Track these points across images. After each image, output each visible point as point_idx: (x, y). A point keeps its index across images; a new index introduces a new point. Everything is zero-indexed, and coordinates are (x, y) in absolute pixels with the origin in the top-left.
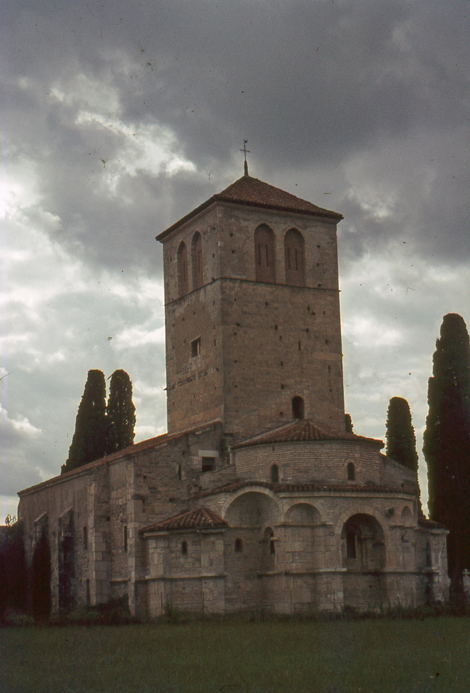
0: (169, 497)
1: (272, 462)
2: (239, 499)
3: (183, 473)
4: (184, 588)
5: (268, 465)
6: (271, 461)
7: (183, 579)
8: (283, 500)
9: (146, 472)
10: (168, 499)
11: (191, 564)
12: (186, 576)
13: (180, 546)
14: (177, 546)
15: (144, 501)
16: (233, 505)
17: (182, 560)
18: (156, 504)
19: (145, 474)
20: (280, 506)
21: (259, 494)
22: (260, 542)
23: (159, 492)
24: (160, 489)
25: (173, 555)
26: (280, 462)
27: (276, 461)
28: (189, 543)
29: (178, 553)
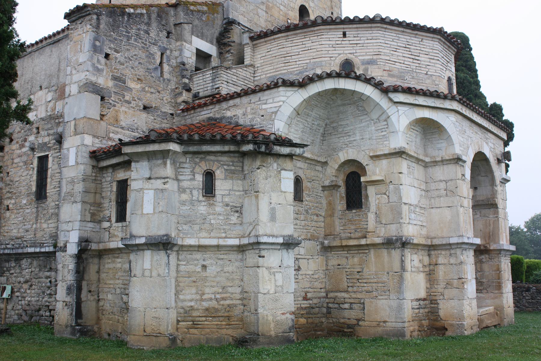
0: (144, 101)
1: (342, 55)
2: (308, 102)
3: (166, 67)
4: (204, 267)
5: (334, 60)
6: (340, 54)
7: (201, 248)
8: (399, 108)
9: (110, 48)
10: (141, 104)
11: (221, 218)
12: (214, 242)
13: (200, 178)
14: (193, 179)
15: (103, 99)
16: (297, 112)
17: (202, 209)
18: (123, 108)
19: (109, 52)
20: (394, 118)
21: (353, 92)
22: (324, 188)
23: (130, 89)
24: (132, 85)
25: (184, 197)
26: (356, 57)
27: (349, 55)
28: (219, 174)
29: (195, 193)
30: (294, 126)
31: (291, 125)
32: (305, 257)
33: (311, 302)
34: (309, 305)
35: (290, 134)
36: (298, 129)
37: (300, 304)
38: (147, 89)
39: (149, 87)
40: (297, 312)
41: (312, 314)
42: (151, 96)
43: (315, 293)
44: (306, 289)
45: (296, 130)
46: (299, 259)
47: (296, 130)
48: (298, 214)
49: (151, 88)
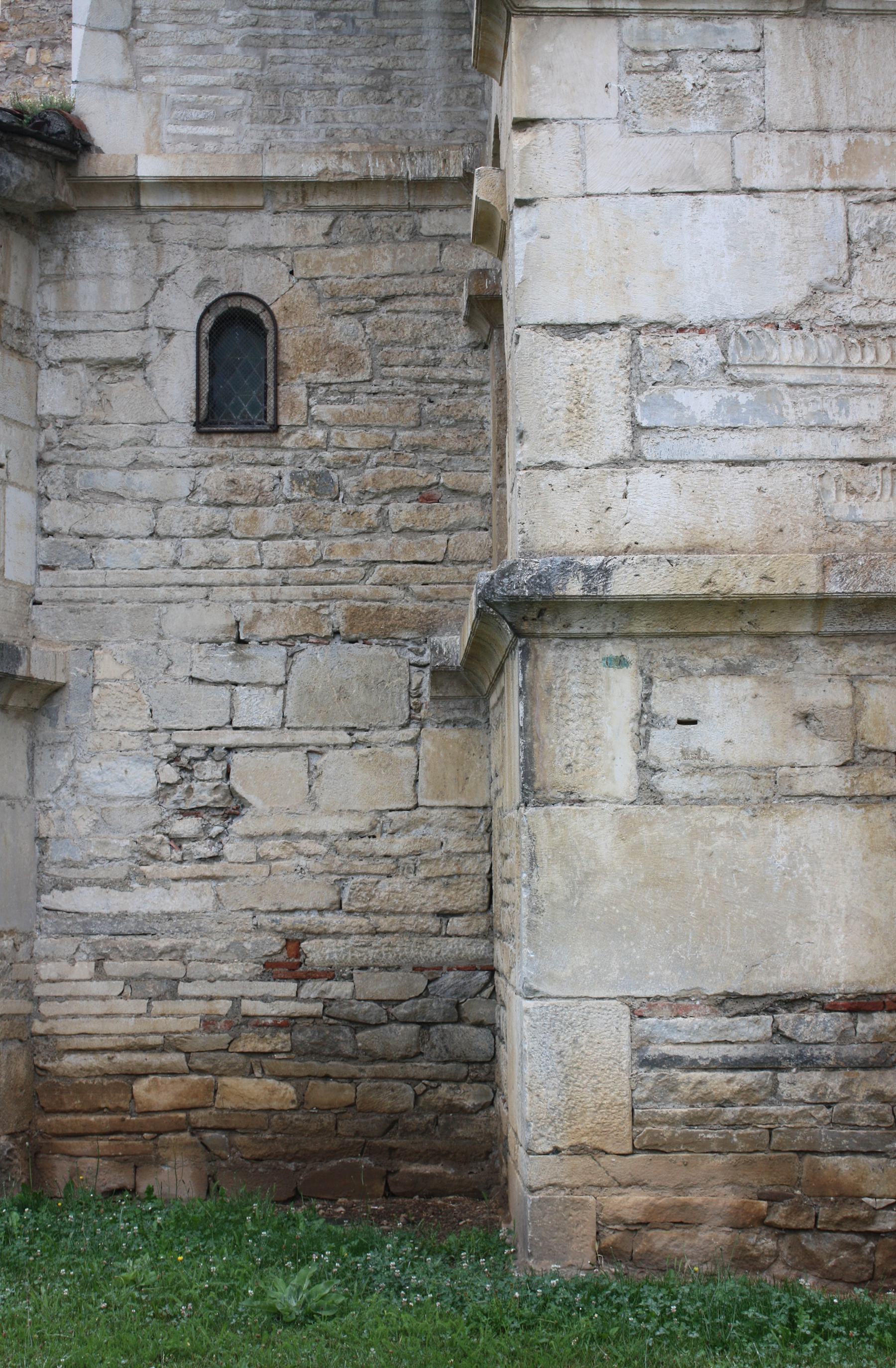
30: (168, 28)
31: (139, 31)
32: (287, 738)
33: (339, 989)
34: (316, 1008)
35: (149, 79)
36: (214, 36)
37: (236, 1000)
38: (30, 58)
39: (42, 45)
40: (202, 1039)
41: (348, 1058)
42: (56, 85)
43: (378, 940)
44: (288, 920)
45: (200, 48)
46: (229, 749)
47: (200, 48)
48: (228, 505)
49: (53, 47)
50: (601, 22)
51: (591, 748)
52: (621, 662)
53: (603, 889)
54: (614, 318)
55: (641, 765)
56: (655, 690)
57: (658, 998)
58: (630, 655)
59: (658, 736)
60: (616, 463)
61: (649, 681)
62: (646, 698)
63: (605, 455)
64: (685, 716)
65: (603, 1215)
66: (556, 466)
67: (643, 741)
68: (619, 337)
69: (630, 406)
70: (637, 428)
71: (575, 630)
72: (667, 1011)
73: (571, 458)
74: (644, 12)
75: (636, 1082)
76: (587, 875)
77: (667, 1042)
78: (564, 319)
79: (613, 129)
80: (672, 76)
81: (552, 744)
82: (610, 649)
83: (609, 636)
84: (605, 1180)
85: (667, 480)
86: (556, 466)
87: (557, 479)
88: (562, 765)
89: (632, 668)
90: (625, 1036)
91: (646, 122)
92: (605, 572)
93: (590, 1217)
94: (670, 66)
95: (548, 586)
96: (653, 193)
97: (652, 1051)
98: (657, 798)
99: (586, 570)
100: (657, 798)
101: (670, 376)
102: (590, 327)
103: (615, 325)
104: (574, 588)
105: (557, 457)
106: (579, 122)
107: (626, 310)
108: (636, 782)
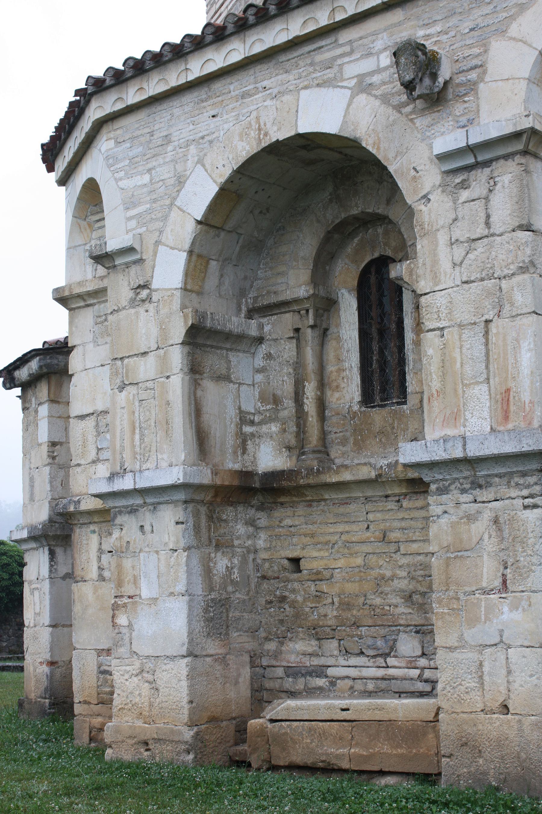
50: (89, 308)
51: (88, 562)
52: (94, 532)
53: (90, 611)
54: (92, 412)
55: (99, 568)
56: (103, 541)
57: (103, 650)
58: (97, 530)
59: (103, 556)
60: (94, 462)
61: (101, 538)
62: (101, 544)
63: (90, 460)
64: (109, 550)
65: (91, 725)
66: (79, 465)
67: (99, 558)
68: (93, 418)
69: (96, 442)
70: (99, 450)
71: (81, 522)
72: (105, 654)
73: (82, 462)
74: (98, 302)
75: (98, 678)
76: (86, 606)
77: (106, 665)
78: (80, 414)
79: (91, 345)
80: (106, 323)
81: (78, 561)
82: (92, 527)
83: (90, 523)
84: (92, 713)
85: (105, 467)
86: (79, 465)
87: (79, 469)
88: (80, 569)
89: (97, 534)
90: (96, 663)
91: (100, 341)
92: (79, 502)
93: (87, 725)
94: (106, 320)
95: (66, 509)
96: (102, 366)
97: (102, 668)
98: (104, 580)
99: (74, 502)
100: (104, 580)
101: (106, 430)
102: (87, 415)
103: (93, 414)
104: (72, 509)
105: (79, 462)
106: (84, 344)
107: (95, 408)
108: (98, 573)
